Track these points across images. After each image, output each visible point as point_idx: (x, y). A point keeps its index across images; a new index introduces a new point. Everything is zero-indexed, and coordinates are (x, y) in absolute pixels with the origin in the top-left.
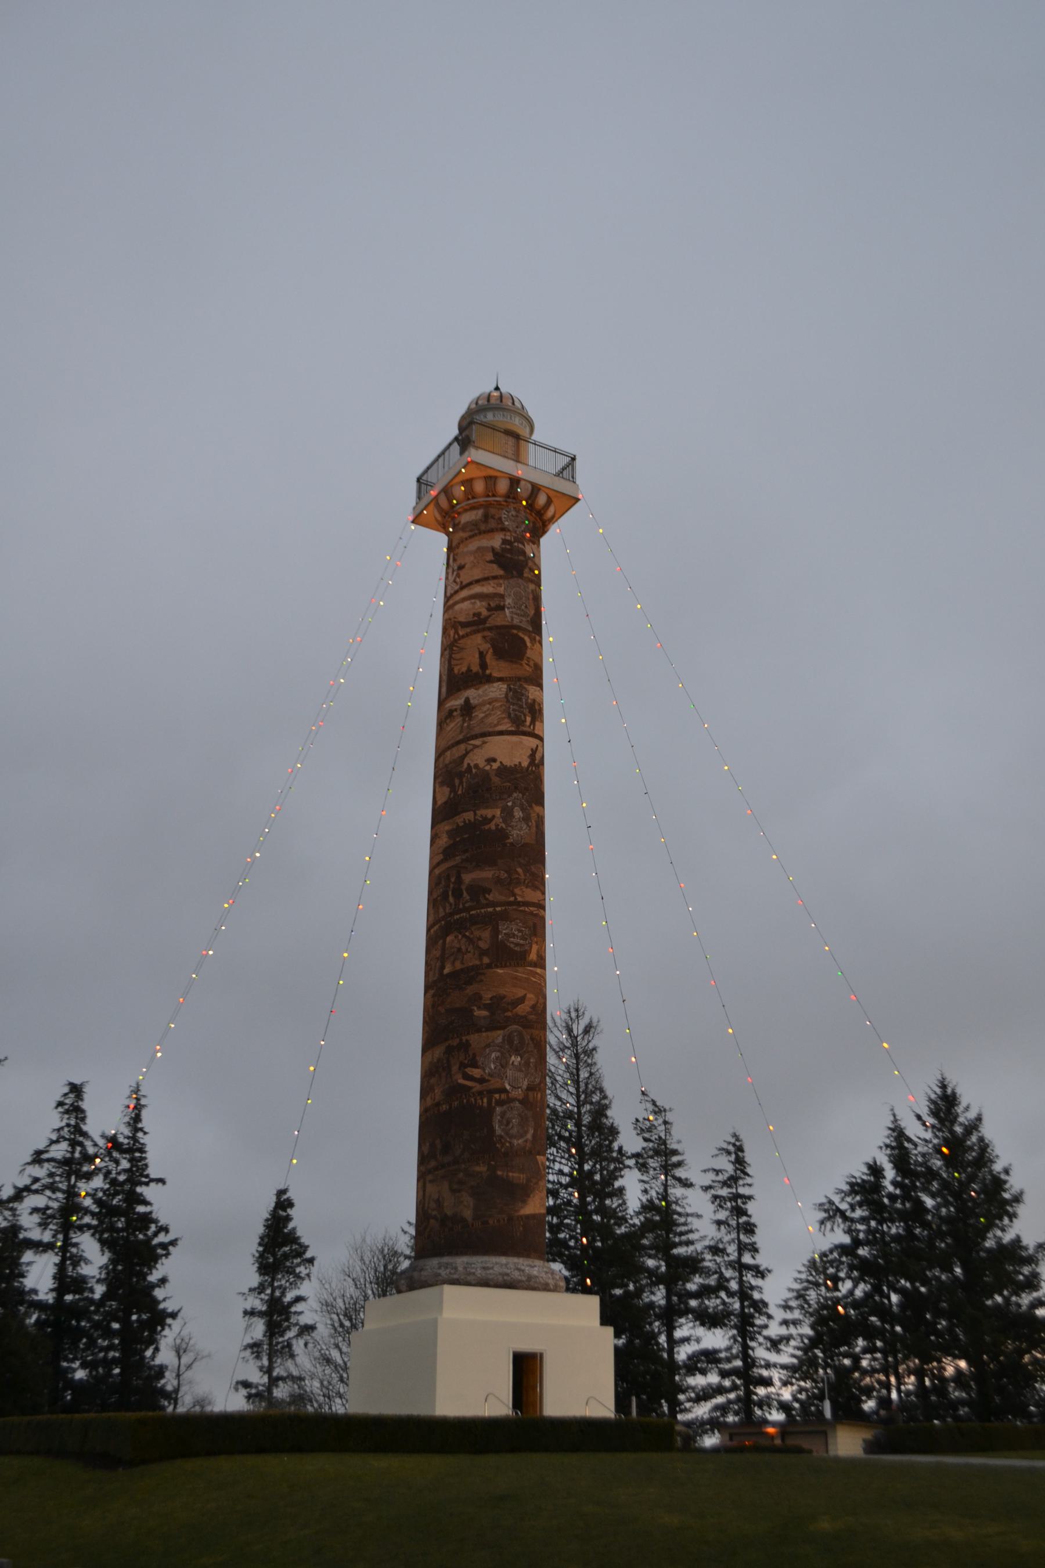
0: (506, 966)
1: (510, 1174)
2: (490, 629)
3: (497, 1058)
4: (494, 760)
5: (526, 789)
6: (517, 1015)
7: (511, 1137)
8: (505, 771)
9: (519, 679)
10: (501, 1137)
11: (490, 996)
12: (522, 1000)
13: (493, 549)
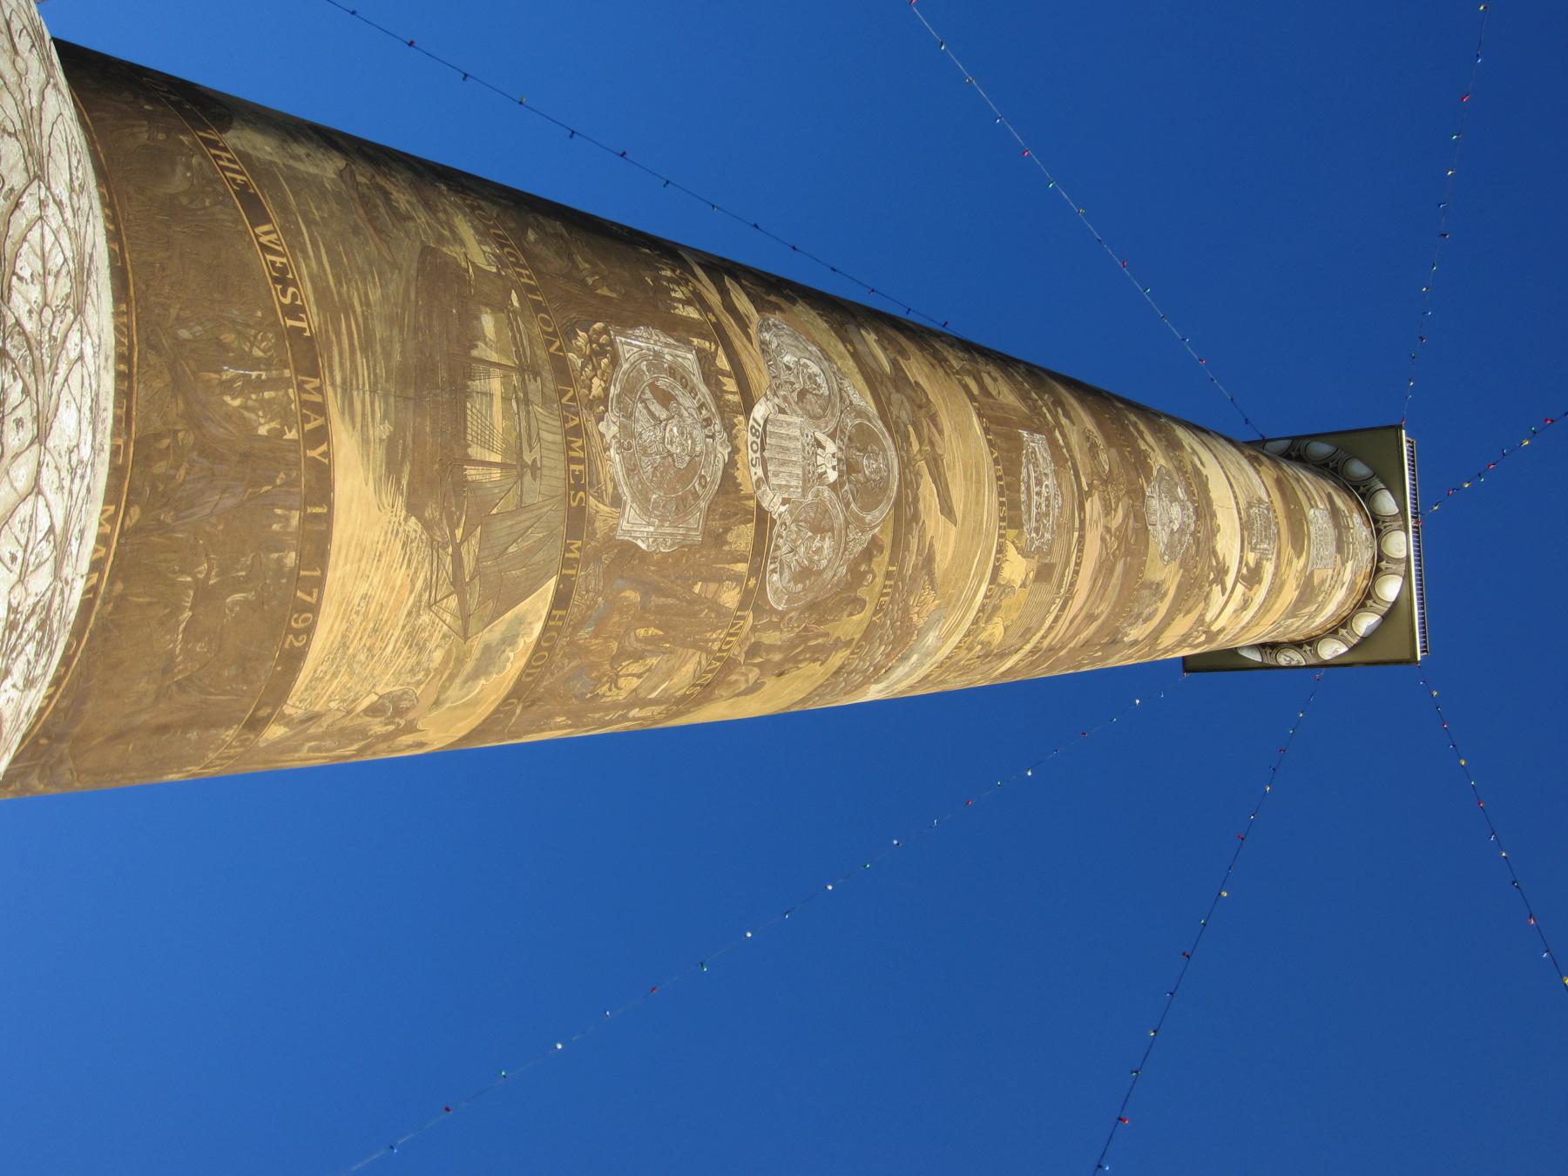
1: (496, 385)
10: (615, 362)
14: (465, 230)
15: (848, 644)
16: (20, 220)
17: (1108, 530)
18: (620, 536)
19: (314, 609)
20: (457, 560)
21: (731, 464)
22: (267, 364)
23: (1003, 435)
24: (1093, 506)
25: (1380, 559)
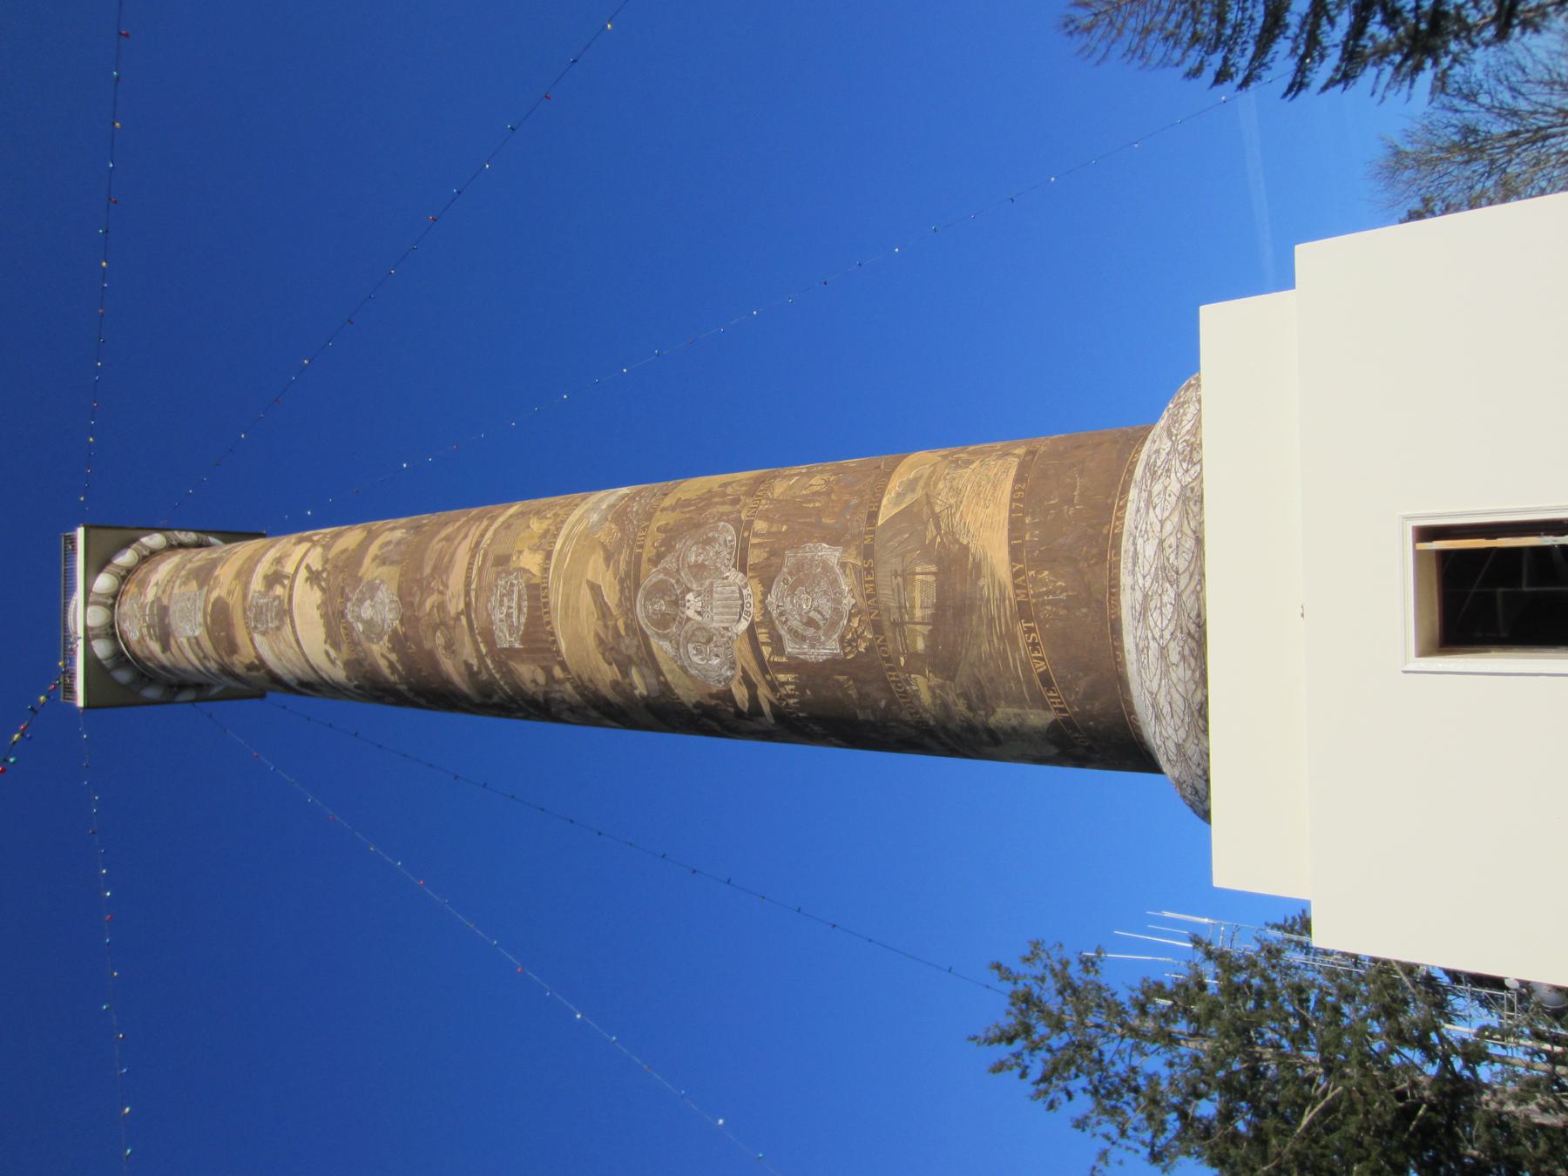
0: (552, 634)
1: (918, 613)
3: (699, 652)
4: (327, 653)
5: (342, 593)
6: (620, 605)
7: (837, 611)
8: (332, 638)
9: (245, 612)
10: (842, 639)
11: (606, 666)
12: (595, 589)
14: (926, 697)
15: (663, 510)
16: (1171, 628)
17: (441, 593)
18: (840, 548)
19: (1012, 500)
20: (938, 527)
21: (765, 595)
22: (1043, 603)
23: (538, 640)
24: (456, 605)
25: (112, 607)
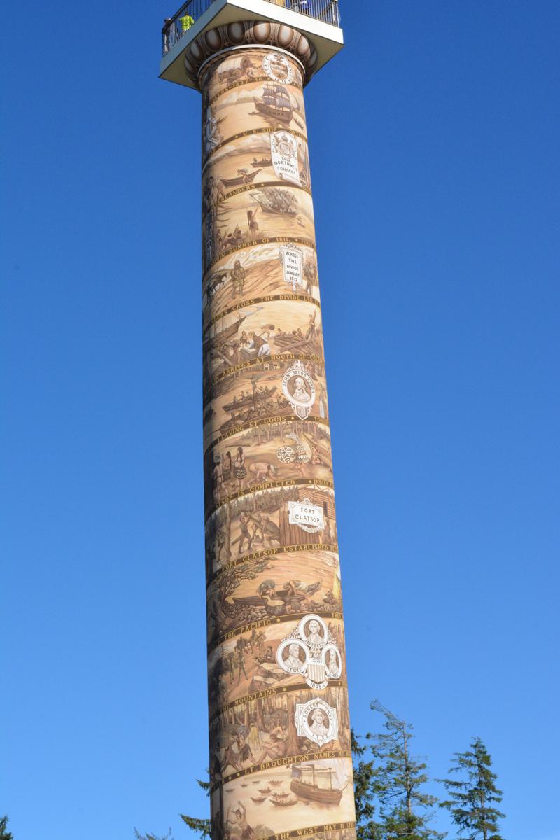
2: (258, 186)
4: (272, 328)
8: (282, 339)
9: (292, 240)
13: (255, 100)
